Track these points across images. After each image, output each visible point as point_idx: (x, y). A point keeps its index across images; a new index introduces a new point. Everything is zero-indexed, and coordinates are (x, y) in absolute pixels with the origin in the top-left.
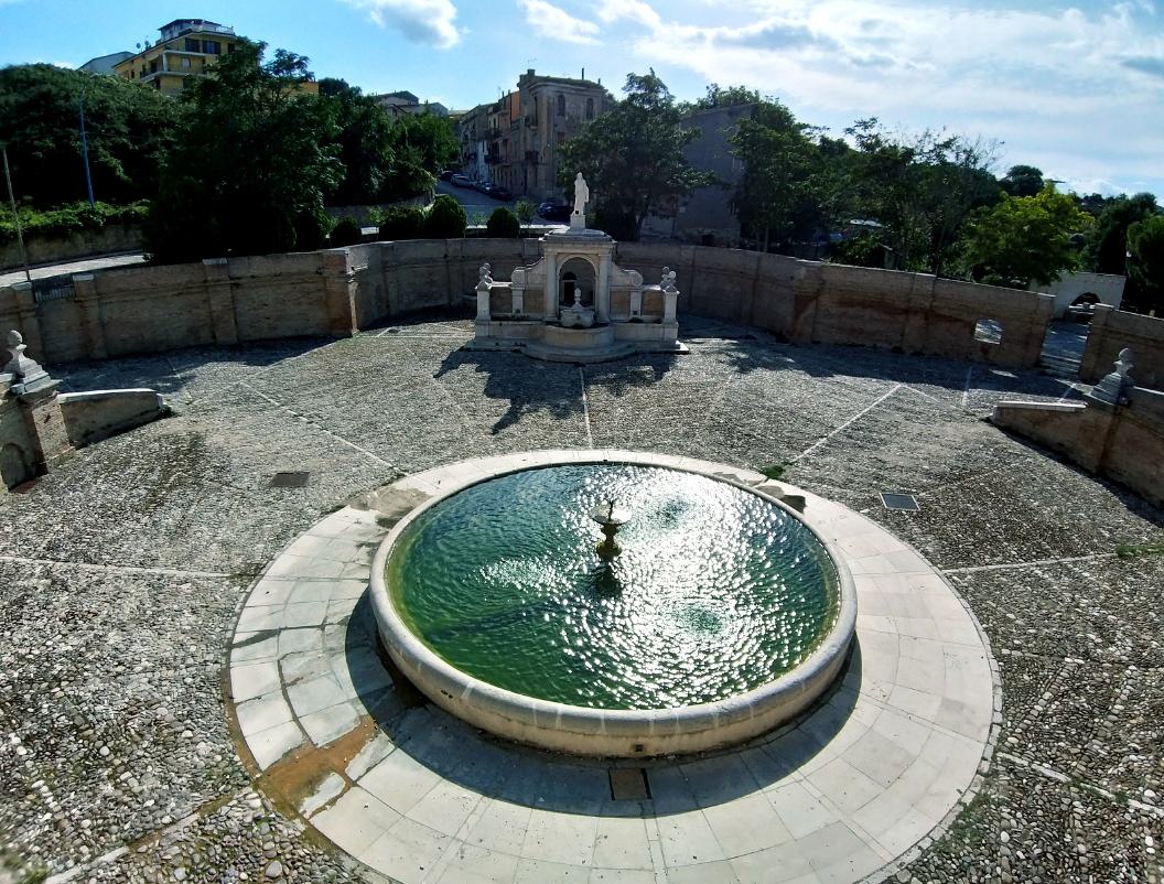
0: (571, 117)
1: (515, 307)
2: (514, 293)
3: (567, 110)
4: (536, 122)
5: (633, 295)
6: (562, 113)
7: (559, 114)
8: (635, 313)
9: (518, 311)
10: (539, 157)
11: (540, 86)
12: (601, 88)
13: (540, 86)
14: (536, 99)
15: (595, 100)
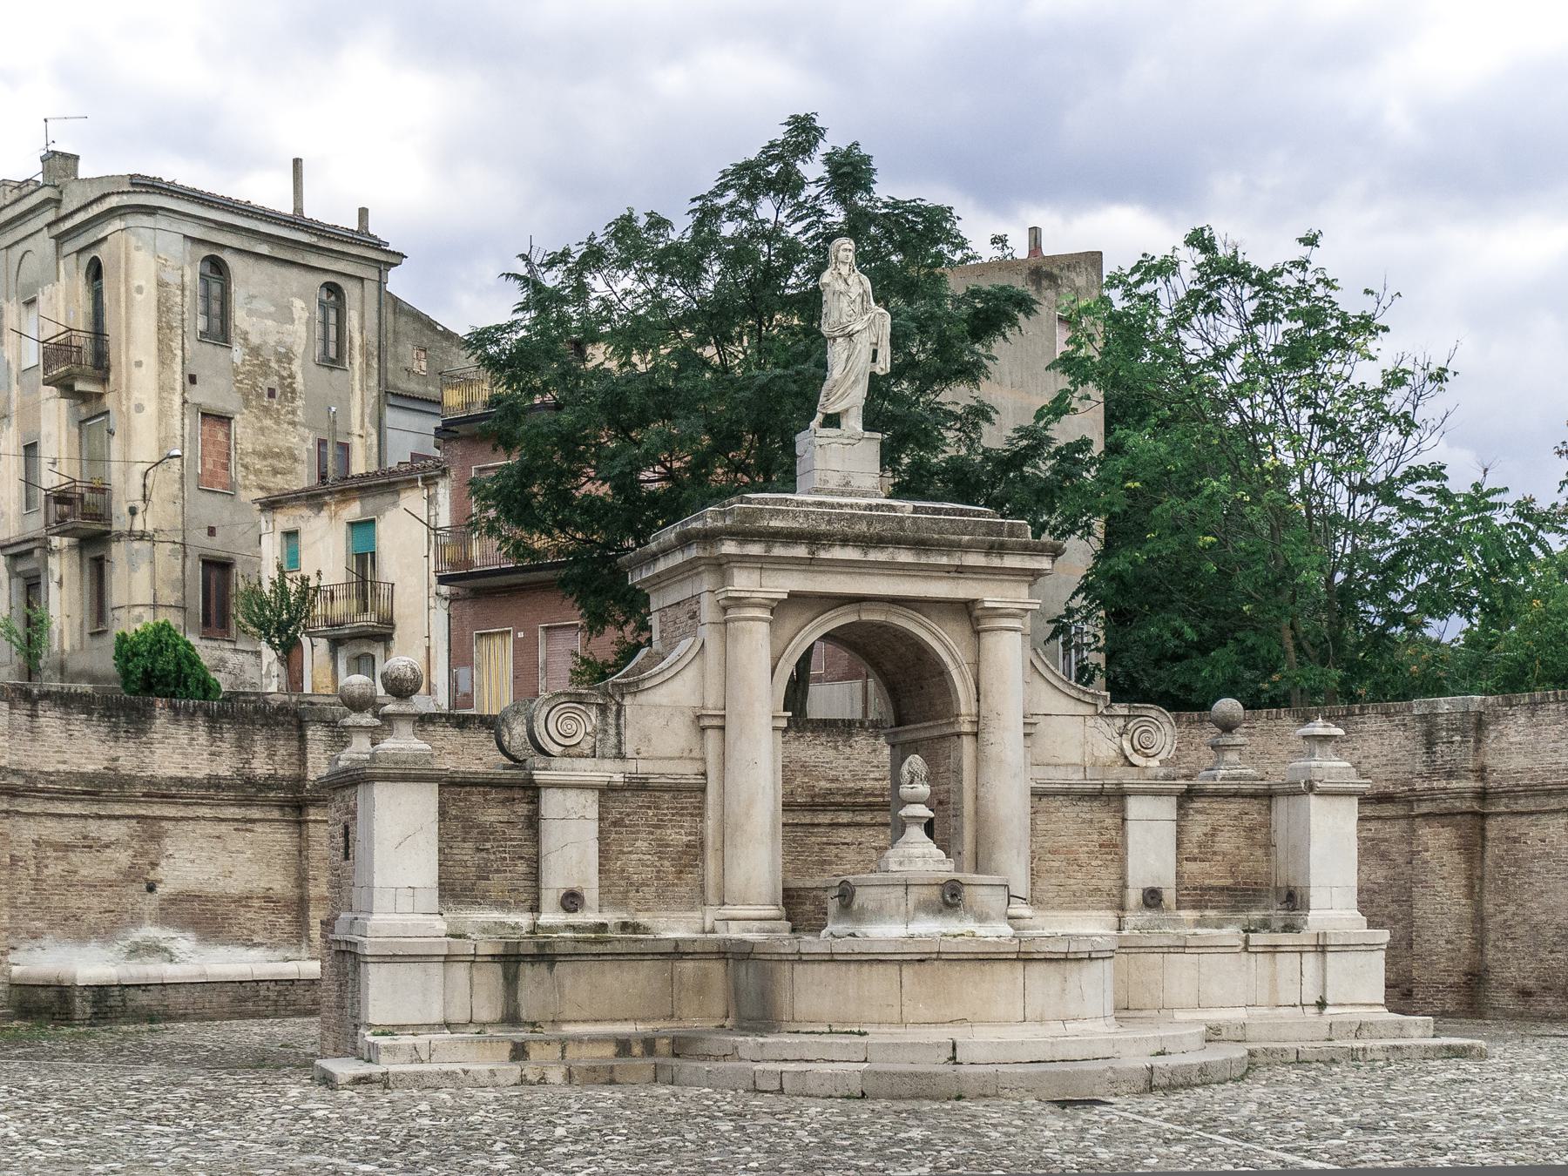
0: (255, 351)
1: (555, 881)
2: (552, 803)
3: (240, 317)
4: (101, 366)
5: (1135, 806)
6: (220, 332)
7: (205, 336)
8: (1152, 898)
9: (571, 901)
10: (120, 509)
11: (112, 213)
12: (378, 245)
13: (112, 213)
14: (95, 271)
15: (351, 290)
